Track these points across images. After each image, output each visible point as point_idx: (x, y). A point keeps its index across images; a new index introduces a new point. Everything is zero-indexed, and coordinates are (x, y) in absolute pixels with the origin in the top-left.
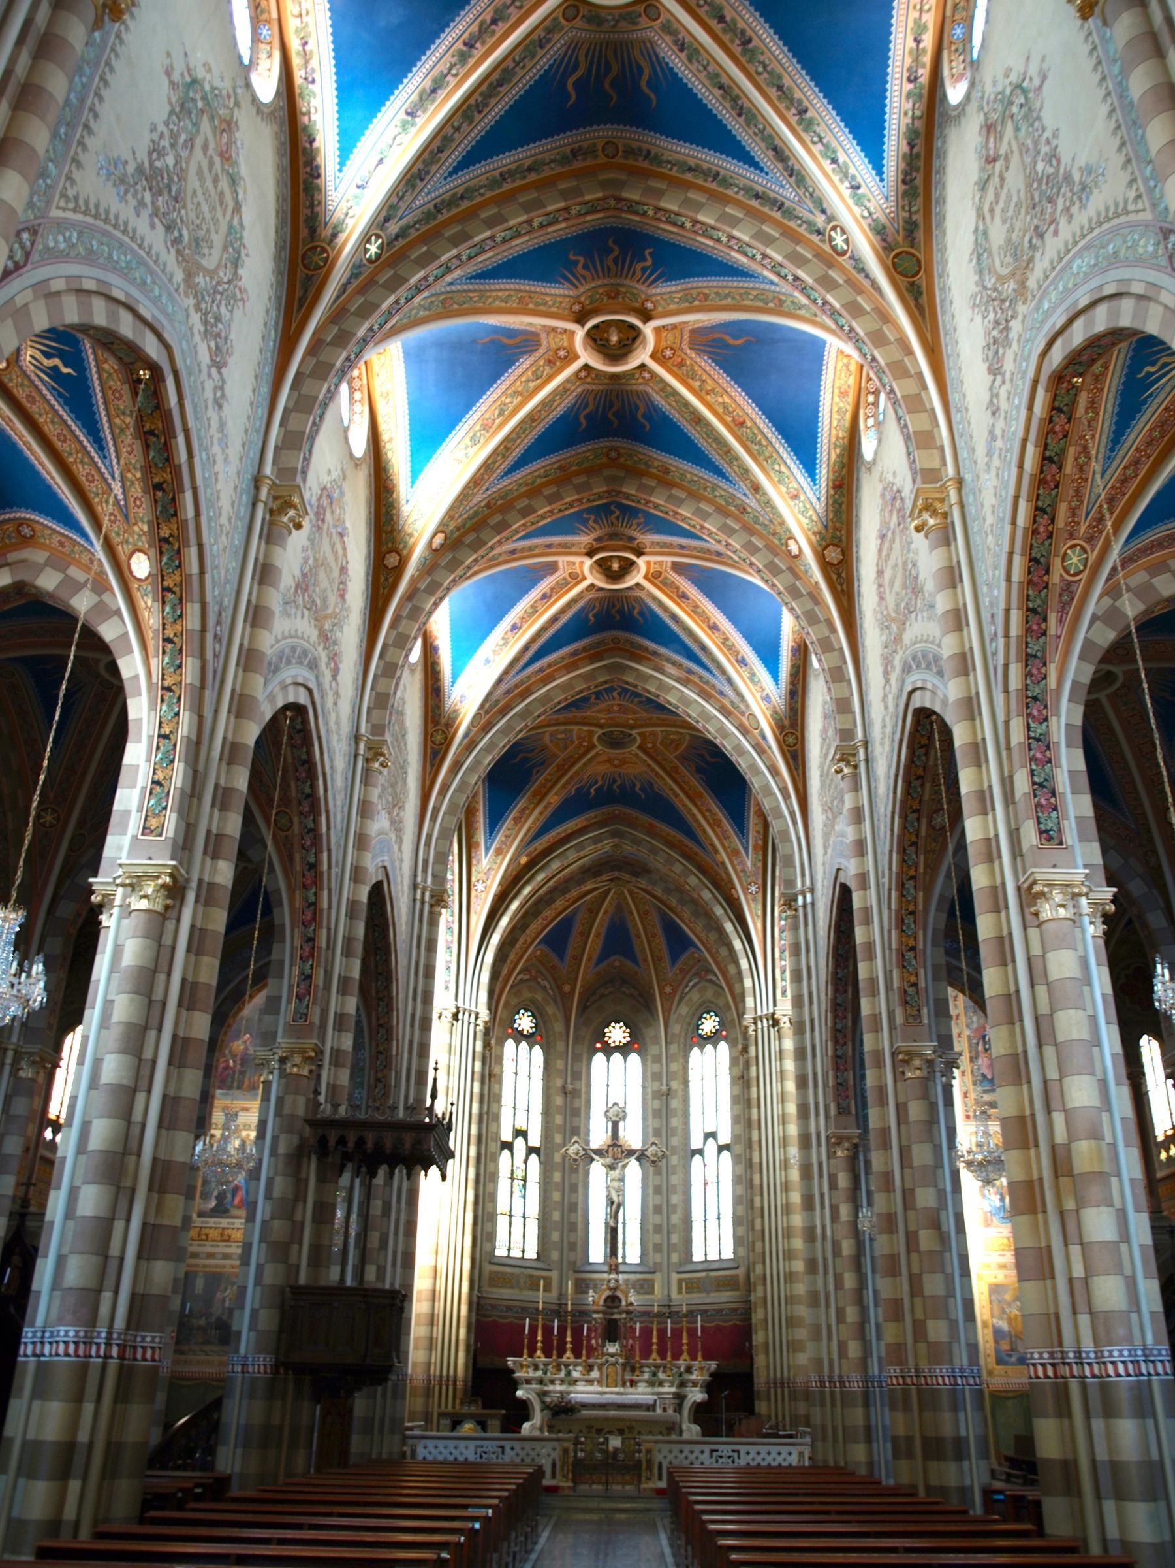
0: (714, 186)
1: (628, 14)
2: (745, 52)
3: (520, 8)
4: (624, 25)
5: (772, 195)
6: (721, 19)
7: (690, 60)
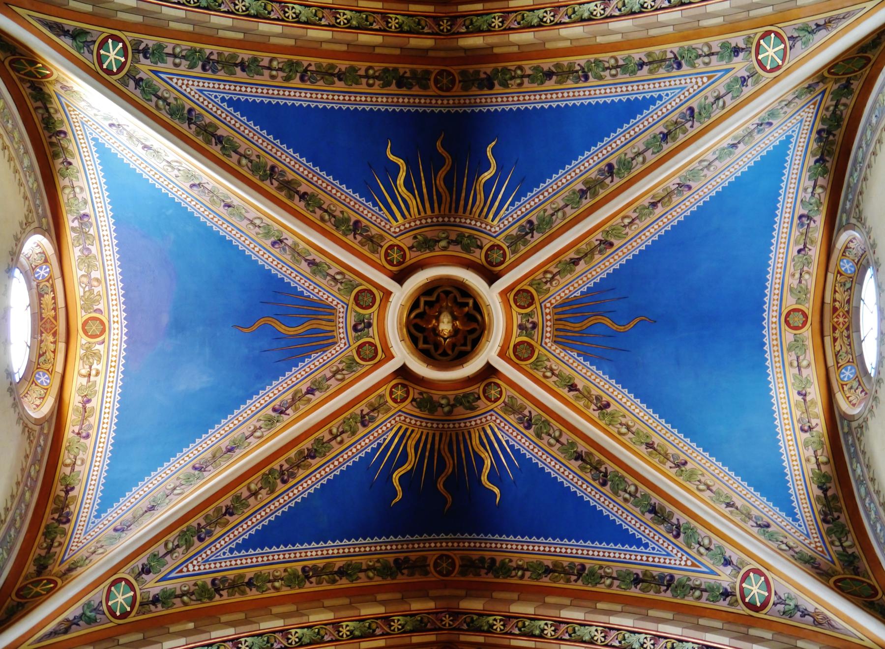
0: (579, 586)
1: (466, 396)
2: (603, 416)
3: (342, 380)
4: (460, 409)
5: (656, 571)
6: (573, 387)
7: (539, 436)
